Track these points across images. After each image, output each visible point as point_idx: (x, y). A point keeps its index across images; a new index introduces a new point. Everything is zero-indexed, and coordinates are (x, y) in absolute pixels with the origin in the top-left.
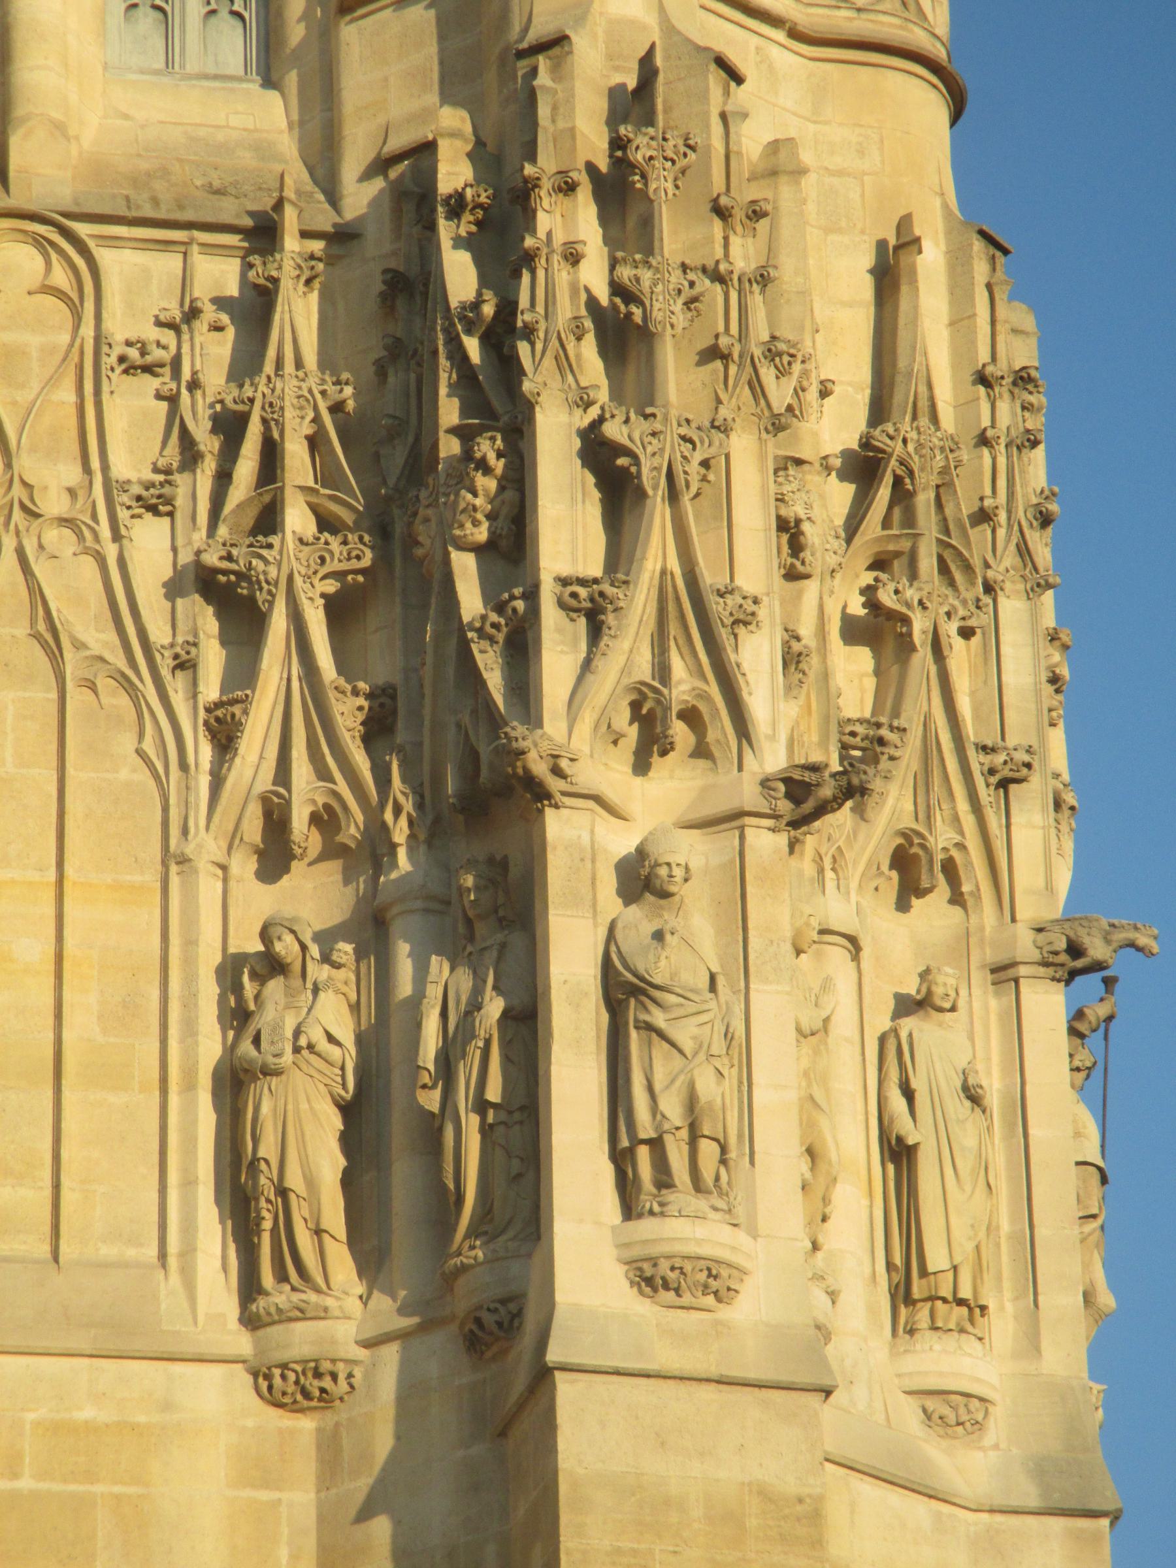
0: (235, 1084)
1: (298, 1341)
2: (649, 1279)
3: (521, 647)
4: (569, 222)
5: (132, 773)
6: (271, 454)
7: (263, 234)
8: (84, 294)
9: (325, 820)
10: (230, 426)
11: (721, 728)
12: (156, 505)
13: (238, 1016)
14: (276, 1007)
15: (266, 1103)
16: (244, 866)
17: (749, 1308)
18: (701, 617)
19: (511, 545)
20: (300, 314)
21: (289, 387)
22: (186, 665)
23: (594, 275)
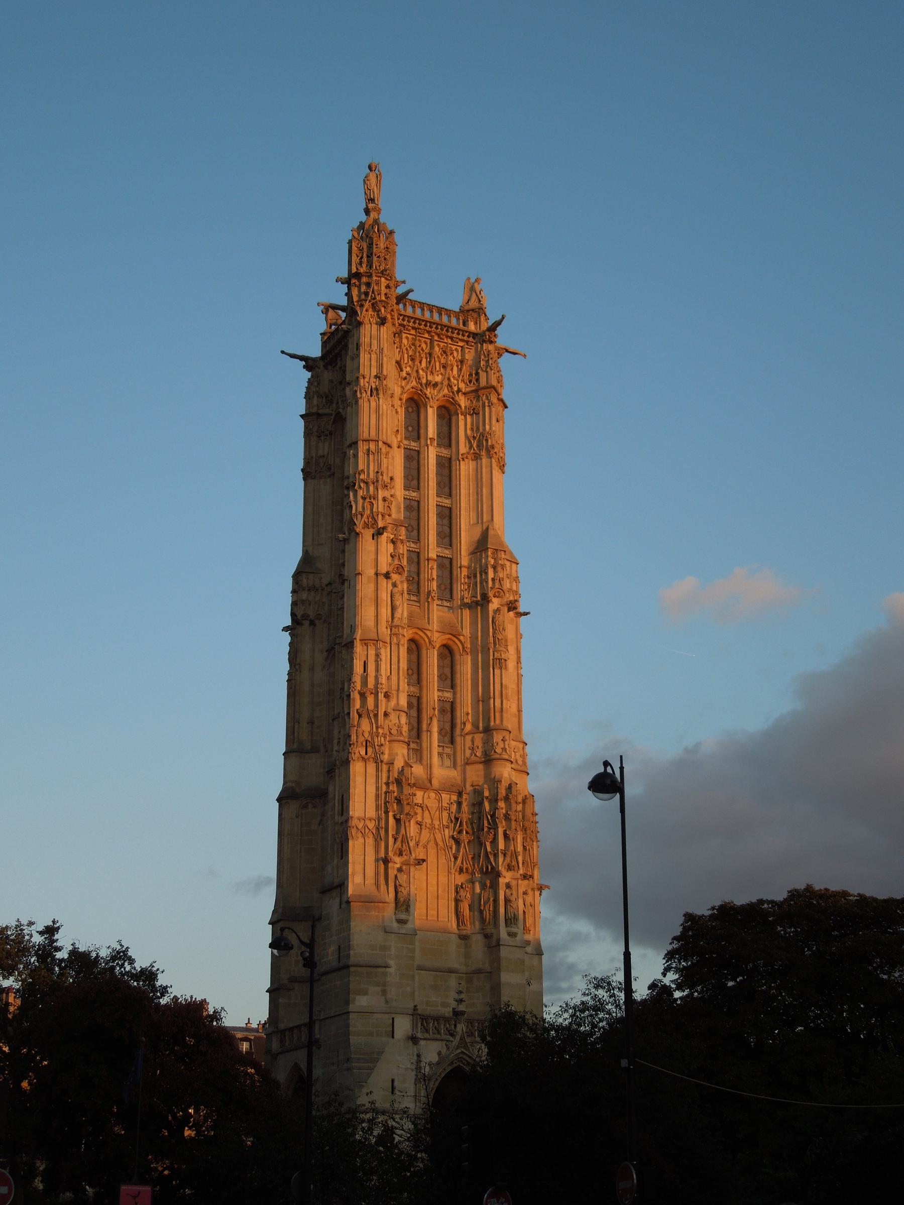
0: (457, 901)
1: (464, 932)
2: (510, 934)
3: (496, 856)
4: (501, 804)
5: (444, 861)
6: (461, 825)
7: (460, 794)
8: (440, 800)
9: (467, 869)
10: (457, 819)
11: (516, 868)
12: (448, 827)
13: (457, 892)
14: (462, 893)
15: (461, 905)
16: (457, 874)
17: (518, 938)
18: (515, 854)
19: (494, 841)
20: (464, 804)
21: (464, 815)
22: (451, 848)
23: (504, 811)
